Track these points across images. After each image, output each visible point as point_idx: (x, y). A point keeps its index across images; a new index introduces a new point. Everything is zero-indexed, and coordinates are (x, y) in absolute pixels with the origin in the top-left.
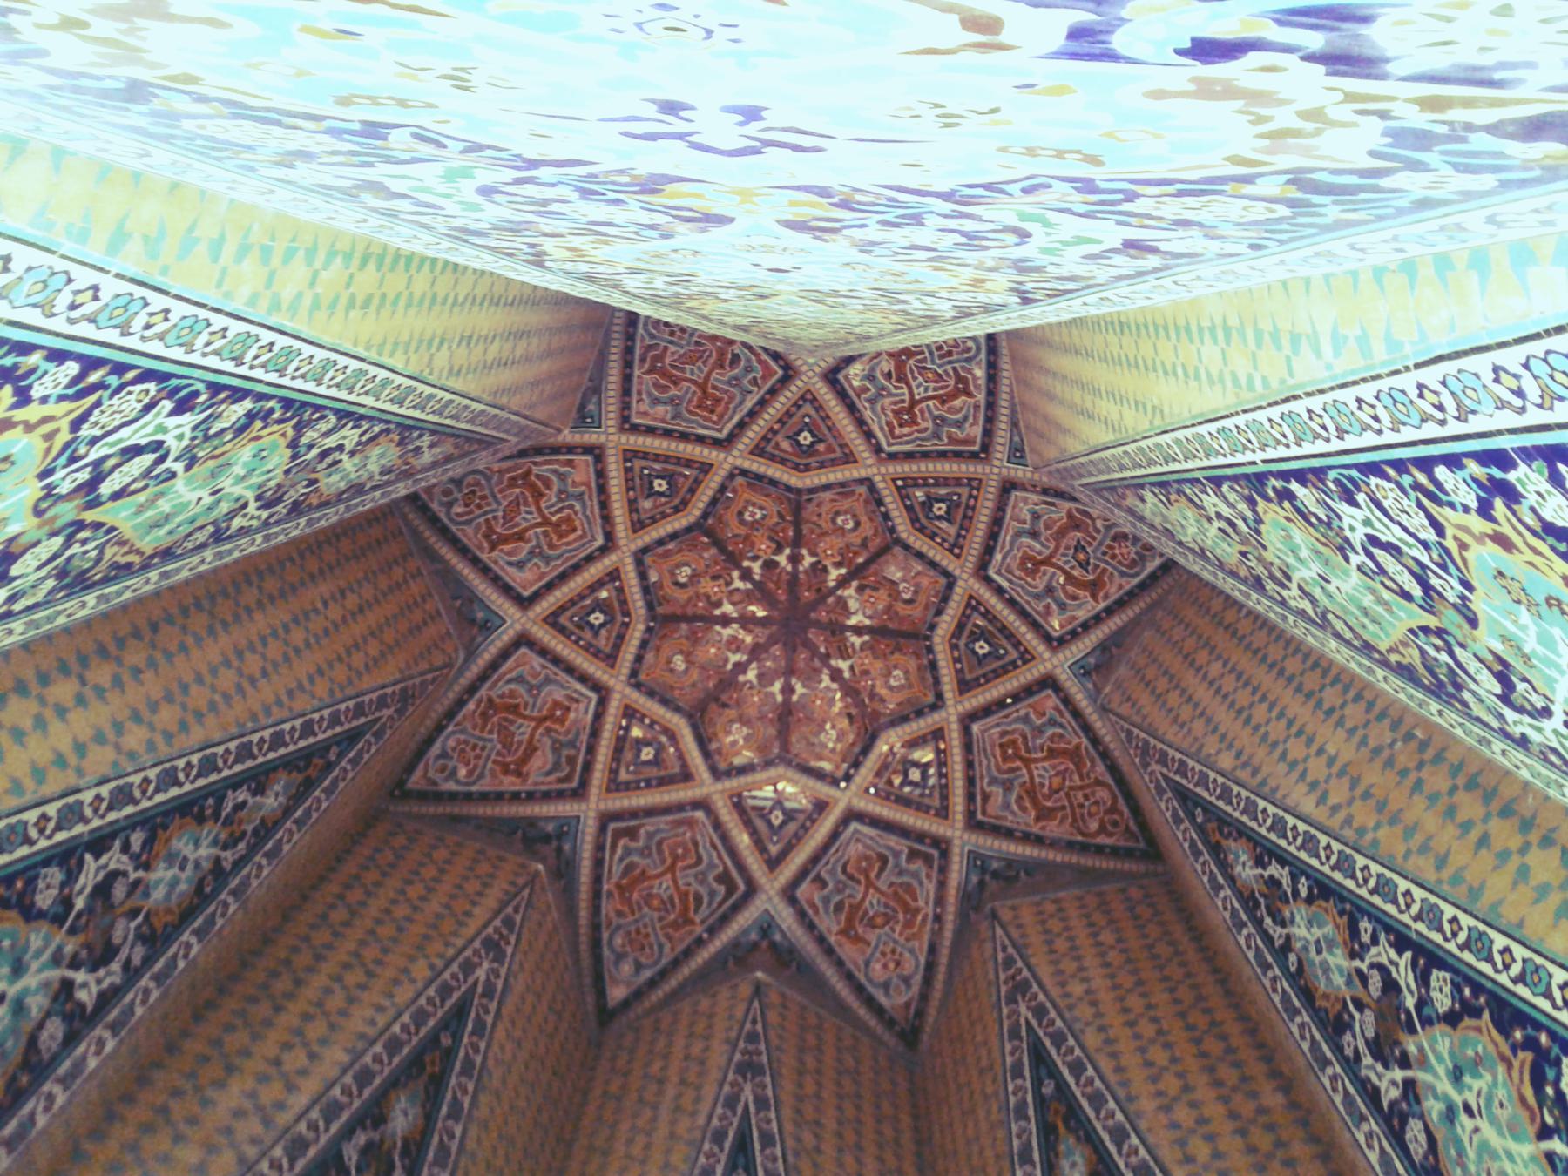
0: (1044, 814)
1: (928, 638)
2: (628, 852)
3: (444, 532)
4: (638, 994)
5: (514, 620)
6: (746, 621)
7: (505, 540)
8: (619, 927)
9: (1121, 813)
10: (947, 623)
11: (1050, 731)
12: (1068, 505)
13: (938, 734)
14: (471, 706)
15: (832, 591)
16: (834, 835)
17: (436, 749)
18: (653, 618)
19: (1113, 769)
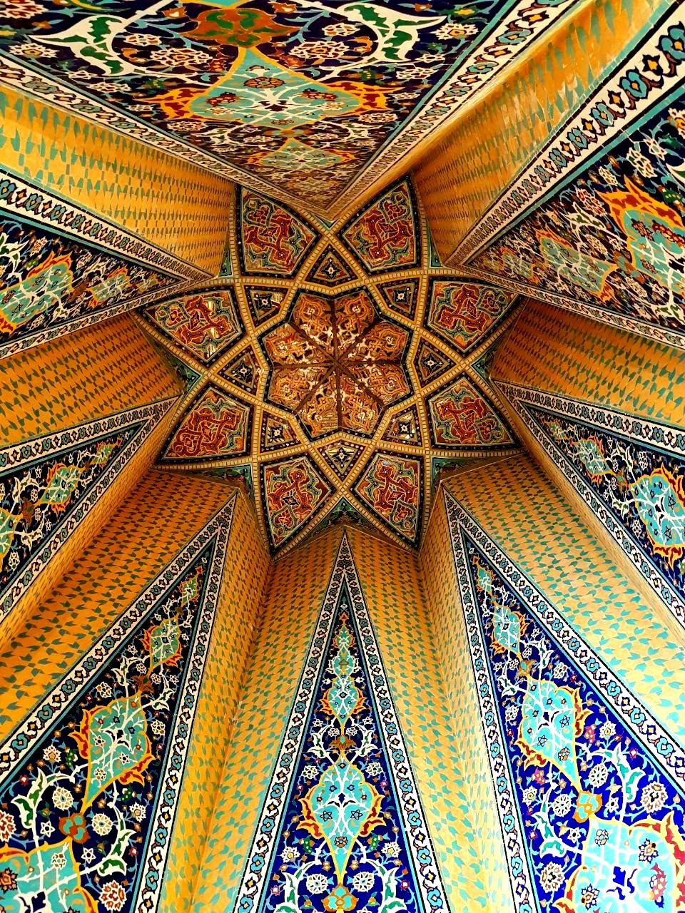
0: (197, 418)
1: (295, 413)
4: (238, 202)
5: (428, 269)
6: (351, 348)
7: (464, 296)
8: (272, 211)
9: (181, 454)
14: (412, 225)
16: (241, 322)
17: (409, 202)
18: (381, 315)
19: (200, 461)
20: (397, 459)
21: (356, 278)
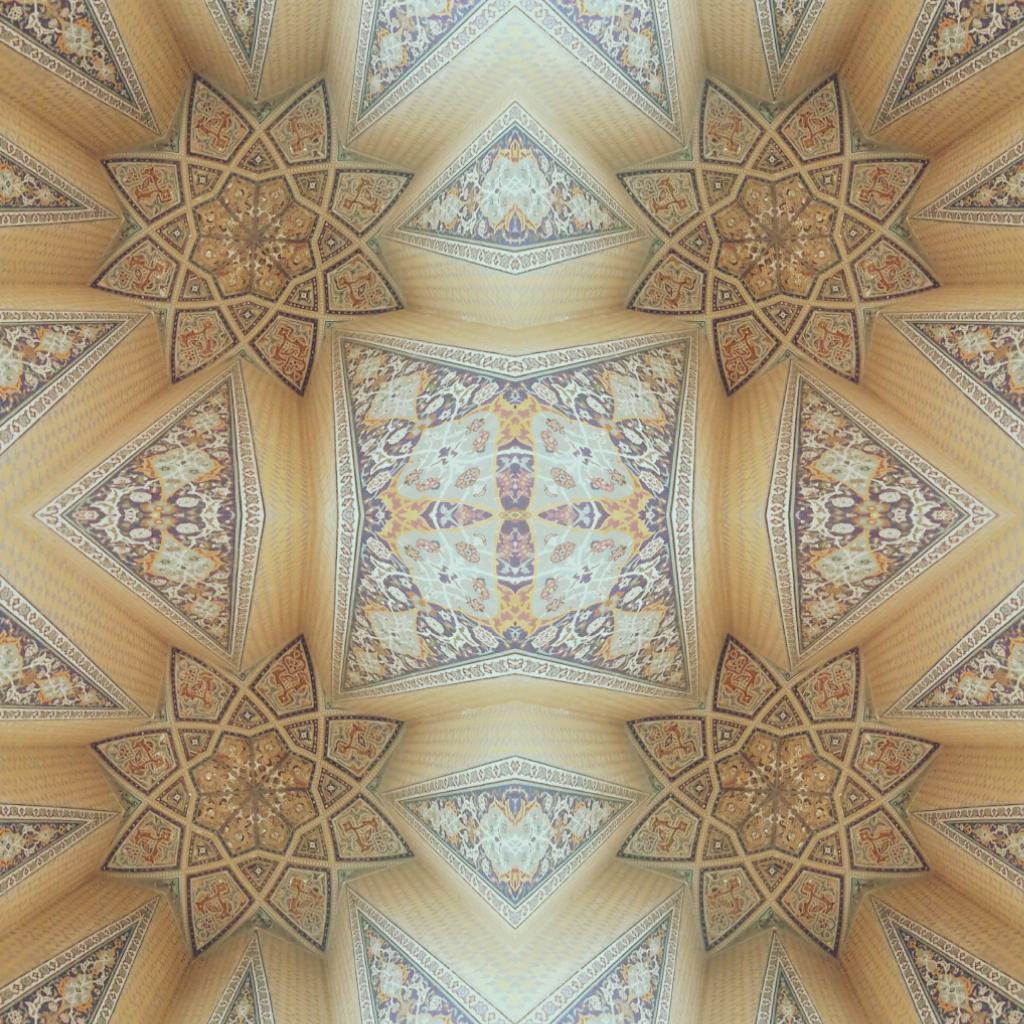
0: (277, 357)
3: (190, 107)
5: (181, 155)
7: (203, 128)
10: (300, 279)
11: (302, 336)
12: (371, 270)
13: (266, 310)
15: (275, 240)
16: (207, 310)
20: (338, 194)
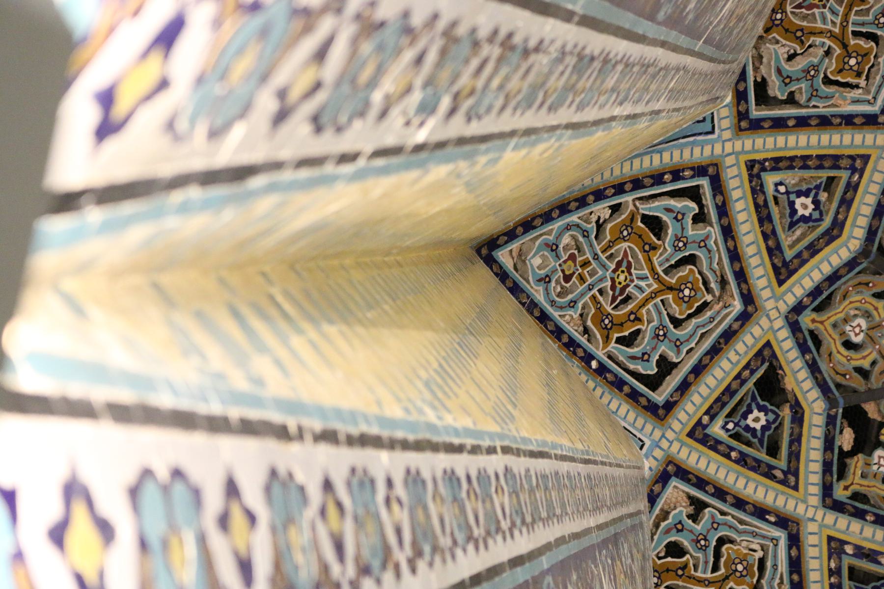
2: (679, 217)
8: (585, 234)
16: (761, 512)
21: (866, 158)
